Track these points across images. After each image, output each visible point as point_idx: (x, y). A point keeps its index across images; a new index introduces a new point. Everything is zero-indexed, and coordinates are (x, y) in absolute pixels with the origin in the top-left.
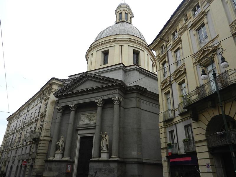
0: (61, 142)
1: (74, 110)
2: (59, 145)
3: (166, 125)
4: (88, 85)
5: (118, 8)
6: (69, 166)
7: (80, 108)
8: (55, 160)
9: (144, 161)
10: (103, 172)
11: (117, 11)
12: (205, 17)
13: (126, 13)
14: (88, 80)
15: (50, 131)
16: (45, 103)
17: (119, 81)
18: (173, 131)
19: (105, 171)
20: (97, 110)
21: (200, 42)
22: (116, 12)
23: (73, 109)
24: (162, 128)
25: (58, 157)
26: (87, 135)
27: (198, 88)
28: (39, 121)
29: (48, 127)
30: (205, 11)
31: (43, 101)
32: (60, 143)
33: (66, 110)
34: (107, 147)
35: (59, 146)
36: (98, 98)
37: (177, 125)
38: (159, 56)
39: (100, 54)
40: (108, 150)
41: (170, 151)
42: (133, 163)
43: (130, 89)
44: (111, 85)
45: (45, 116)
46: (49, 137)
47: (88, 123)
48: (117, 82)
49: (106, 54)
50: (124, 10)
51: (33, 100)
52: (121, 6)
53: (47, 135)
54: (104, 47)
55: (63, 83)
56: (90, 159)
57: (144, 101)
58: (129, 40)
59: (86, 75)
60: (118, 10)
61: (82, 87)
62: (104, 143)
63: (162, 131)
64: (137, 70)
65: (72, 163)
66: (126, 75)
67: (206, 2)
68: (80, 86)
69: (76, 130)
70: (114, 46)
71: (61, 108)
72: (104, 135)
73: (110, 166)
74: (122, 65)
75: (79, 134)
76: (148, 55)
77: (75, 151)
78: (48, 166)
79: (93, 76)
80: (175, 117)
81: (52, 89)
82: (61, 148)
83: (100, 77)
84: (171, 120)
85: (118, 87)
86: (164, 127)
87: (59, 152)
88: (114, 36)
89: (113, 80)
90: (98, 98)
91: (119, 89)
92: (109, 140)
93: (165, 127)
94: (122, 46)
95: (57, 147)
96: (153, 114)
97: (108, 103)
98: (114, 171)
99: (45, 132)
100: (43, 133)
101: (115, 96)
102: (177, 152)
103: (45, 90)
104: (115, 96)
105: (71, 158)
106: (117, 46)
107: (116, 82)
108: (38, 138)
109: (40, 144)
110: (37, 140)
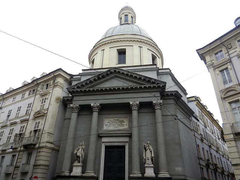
1: (76, 111)
2: (78, 154)
3: (235, 138)
4: (115, 83)
7: (105, 109)
8: (74, 175)
11: (122, 12)
14: (116, 76)
15: (53, 136)
16: (41, 99)
20: (131, 113)
25: (77, 171)
26: (116, 143)
28: (30, 122)
29: (52, 131)
31: (38, 96)
32: (80, 153)
36: (134, 100)
38: (213, 62)
39: (114, 53)
40: (152, 164)
43: (167, 95)
44: (152, 86)
47: (116, 128)
48: (161, 84)
49: (122, 53)
50: (130, 13)
51: (10, 96)
52: (127, 8)
53: (51, 141)
54: (121, 45)
55: (70, 77)
59: (115, 71)
60: (122, 12)
68: (104, 83)
69: (100, 137)
70: (133, 46)
74: (155, 67)
75: (103, 142)
79: (125, 73)
82: (81, 159)
83: (136, 76)
88: (133, 36)
89: (155, 81)
90: (134, 100)
94: (140, 47)
95: (75, 158)
99: (47, 137)
100: (45, 138)
101: (156, 100)
104: (156, 100)
106: (136, 47)
108: (35, 145)
109: (40, 152)
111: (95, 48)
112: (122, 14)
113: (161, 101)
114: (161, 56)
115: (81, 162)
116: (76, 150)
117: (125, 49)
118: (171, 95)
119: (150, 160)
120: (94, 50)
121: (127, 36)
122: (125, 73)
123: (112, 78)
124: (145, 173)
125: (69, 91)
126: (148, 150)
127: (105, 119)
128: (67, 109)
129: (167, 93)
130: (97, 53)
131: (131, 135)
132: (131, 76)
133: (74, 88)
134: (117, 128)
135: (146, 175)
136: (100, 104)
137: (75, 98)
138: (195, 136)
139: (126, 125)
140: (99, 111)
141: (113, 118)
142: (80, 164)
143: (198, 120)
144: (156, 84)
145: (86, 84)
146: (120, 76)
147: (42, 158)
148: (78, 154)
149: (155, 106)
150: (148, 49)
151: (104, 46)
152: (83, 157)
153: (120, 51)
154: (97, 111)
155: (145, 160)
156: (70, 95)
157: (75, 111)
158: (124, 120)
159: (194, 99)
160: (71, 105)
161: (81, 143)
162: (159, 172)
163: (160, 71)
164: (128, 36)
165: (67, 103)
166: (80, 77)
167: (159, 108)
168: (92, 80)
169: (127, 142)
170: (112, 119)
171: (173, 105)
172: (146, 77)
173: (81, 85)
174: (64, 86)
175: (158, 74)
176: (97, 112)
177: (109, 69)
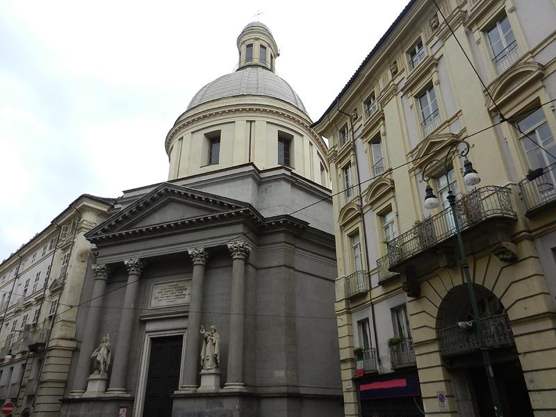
0: (103, 351)
1: (135, 273)
4: (171, 214)
6: (121, 410)
7: (152, 269)
9: (303, 391)
12: (434, 69)
13: (261, 46)
14: (171, 201)
15: (75, 325)
16: (63, 256)
18: (367, 319)
20: (192, 272)
21: (424, 123)
22: (240, 42)
23: (133, 271)
24: (343, 314)
26: (168, 332)
27: (419, 224)
28: (45, 303)
29: (71, 315)
30: (433, 56)
31: (59, 251)
33: (116, 273)
34: (216, 360)
35: (99, 363)
36: (195, 246)
37: (375, 306)
40: (217, 367)
41: (360, 365)
42: (276, 397)
44: (225, 213)
45: (62, 289)
46: (71, 339)
47: (171, 303)
48: (241, 208)
50: (257, 39)
52: (250, 29)
54: (210, 125)
56: (176, 392)
57: (301, 251)
58: (268, 109)
59: (166, 190)
61: (157, 219)
62: (209, 351)
63: (342, 320)
64: (285, 180)
65: (131, 401)
66: (260, 191)
67: (436, 38)
71: (103, 269)
72: (210, 333)
74: (251, 168)
75: (147, 332)
76: (311, 144)
77: (138, 374)
78: (69, 413)
79: (183, 192)
80: (371, 289)
81: (82, 222)
82: (102, 366)
83: (200, 196)
84: (363, 295)
85: (241, 220)
86: (347, 312)
87: (99, 376)
88: (234, 99)
91: (244, 223)
92: (220, 345)
93: (349, 312)
94: (251, 122)
95: (93, 366)
96: (322, 280)
97: (218, 257)
100: (58, 331)
102: (376, 367)
103: (63, 224)
104: (234, 238)
105: (127, 391)
106: (241, 123)
107: (237, 207)
108: (43, 345)
109: (48, 357)
110: (40, 348)
121: (224, 101)
122: (183, 192)
123: (164, 205)
132: (193, 196)
147: (49, 368)
149: (192, 258)
150: (267, 122)
163: (263, 175)
164: (227, 100)
170: (166, 286)
171: (283, 244)
172: (215, 196)
177: (154, 188)
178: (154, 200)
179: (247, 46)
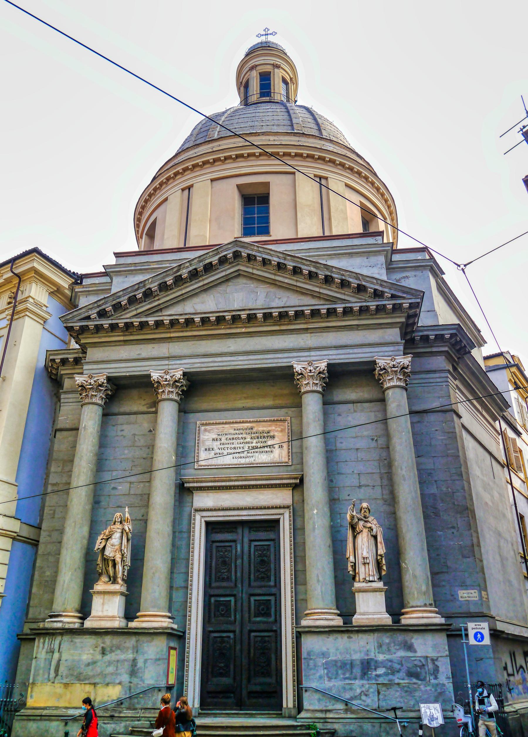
2: (109, 552)
5: (247, 55)
10: (378, 676)
11: (251, 63)
17: (412, 295)
19: (393, 671)
40: (380, 579)
43: (425, 339)
47: (243, 461)
48: (404, 298)
55: (71, 281)
59: (237, 255)
60: (251, 63)
73: (415, 651)
75: (196, 510)
81: (25, 300)
82: (119, 568)
85: (398, 320)
92: (386, 541)
94: (321, 178)
98: (436, 670)
111: (156, 184)
112: (252, 68)
113: (406, 360)
114: (391, 213)
115: (120, 580)
116: (100, 538)
117: (267, 185)
118: (440, 338)
119: (372, 567)
120: (155, 190)
123: (227, 280)
124: (354, 613)
125: (70, 329)
126: (365, 531)
127: (203, 428)
128: (62, 396)
129: (425, 333)
130: (166, 199)
131: (298, 481)
133: (88, 318)
134: (247, 460)
135: (358, 619)
136: (185, 374)
137: (93, 354)
138: (511, 484)
139: (281, 447)
140: (181, 399)
141: (233, 423)
142: (116, 587)
143: (519, 434)
144: (388, 299)
145: (132, 300)
146: (255, 272)
148: (109, 552)
151: (189, 175)
152: (128, 562)
153: (249, 191)
154: (174, 396)
155: (354, 570)
156: (74, 345)
157: (94, 400)
158: (270, 428)
159: (500, 361)
160: (79, 379)
161: (118, 514)
162: (403, 607)
165: (62, 372)
166: (106, 279)
167: (398, 383)
168: (154, 286)
169: (288, 507)
173: (114, 306)
174: (50, 315)
175: (390, 267)
176: (175, 401)
178: (209, 268)
179: (261, 74)
